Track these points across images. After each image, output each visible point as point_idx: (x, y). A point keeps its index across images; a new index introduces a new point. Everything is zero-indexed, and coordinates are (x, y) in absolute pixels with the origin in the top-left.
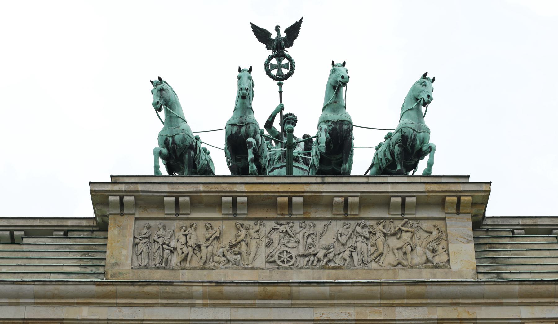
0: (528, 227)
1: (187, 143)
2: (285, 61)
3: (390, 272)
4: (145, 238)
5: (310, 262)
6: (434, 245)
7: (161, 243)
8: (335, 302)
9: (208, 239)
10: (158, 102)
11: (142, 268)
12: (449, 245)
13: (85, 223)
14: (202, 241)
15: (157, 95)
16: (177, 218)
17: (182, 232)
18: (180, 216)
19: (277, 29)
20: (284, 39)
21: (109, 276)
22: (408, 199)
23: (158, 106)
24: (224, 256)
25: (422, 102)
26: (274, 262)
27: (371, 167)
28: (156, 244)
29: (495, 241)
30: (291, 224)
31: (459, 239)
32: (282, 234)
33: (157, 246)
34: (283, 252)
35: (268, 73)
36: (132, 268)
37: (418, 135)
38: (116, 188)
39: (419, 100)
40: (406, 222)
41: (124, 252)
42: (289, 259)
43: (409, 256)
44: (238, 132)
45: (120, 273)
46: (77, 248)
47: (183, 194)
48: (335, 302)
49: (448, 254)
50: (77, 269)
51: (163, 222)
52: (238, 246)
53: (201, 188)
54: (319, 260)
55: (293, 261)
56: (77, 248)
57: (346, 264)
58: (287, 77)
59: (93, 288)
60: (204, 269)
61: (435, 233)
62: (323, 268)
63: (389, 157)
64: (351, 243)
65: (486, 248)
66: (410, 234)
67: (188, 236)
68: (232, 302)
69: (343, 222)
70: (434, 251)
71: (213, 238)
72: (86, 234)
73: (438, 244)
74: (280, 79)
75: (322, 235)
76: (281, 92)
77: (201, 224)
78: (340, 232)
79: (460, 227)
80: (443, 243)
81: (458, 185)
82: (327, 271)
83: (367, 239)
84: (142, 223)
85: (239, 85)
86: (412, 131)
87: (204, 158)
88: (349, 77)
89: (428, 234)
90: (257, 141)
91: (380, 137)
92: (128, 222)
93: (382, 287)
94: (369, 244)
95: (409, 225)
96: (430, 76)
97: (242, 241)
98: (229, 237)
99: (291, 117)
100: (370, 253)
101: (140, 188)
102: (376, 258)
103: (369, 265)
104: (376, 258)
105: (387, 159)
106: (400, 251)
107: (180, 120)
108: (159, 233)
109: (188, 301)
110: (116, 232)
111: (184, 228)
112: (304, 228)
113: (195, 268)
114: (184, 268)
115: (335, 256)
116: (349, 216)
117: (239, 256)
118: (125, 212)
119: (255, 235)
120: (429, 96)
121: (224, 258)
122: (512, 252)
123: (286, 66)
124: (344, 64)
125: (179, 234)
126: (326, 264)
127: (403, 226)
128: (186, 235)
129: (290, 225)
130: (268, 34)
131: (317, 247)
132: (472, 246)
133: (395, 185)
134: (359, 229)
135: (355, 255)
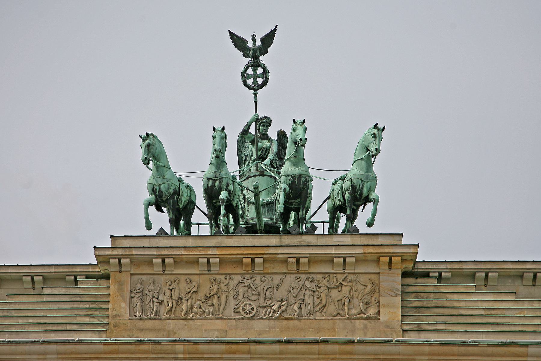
1: (171, 191)
2: (260, 71)
3: (331, 322)
7: (151, 297)
8: (283, 356)
9: (189, 293)
10: (146, 158)
11: (138, 319)
15: (145, 151)
17: (168, 287)
19: (254, 39)
20: (260, 48)
22: (348, 260)
23: (147, 162)
24: (200, 307)
27: (329, 198)
28: (148, 297)
30: (254, 279)
31: (389, 292)
32: (246, 288)
33: (148, 299)
34: (247, 304)
35: (245, 83)
36: (130, 319)
38: (115, 252)
40: (346, 277)
42: (251, 310)
43: (346, 308)
44: (213, 185)
47: (169, 257)
48: (283, 356)
49: (379, 306)
51: (152, 276)
52: (212, 298)
53: (182, 252)
54: (274, 311)
55: (254, 312)
57: (295, 316)
59: (102, 347)
60: (184, 319)
61: (369, 286)
62: (278, 319)
65: (412, 297)
66: (348, 288)
67: (173, 291)
68: (205, 356)
69: (296, 275)
70: (367, 303)
71: (192, 292)
74: (256, 88)
75: (278, 288)
76: (256, 102)
77: (183, 278)
78: (292, 286)
80: (376, 295)
83: (314, 292)
84: (136, 278)
87: (185, 196)
89: (365, 287)
90: (229, 192)
93: (319, 346)
94: (315, 295)
95: (348, 280)
97: (215, 294)
100: (315, 304)
101: (134, 252)
102: (320, 309)
103: (314, 314)
104: (320, 309)
105: (339, 201)
106: (340, 302)
107: (165, 169)
108: (149, 288)
109: (172, 356)
111: (169, 283)
112: (264, 282)
113: (178, 319)
114: (170, 319)
116: (300, 272)
117: (212, 307)
118: (123, 269)
119: (225, 289)
121: (200, 310)
123: (261, 76)
125: (165, 289)
128: (171, 290)
129: (252, 280)
130: (244, 42)
131: (274, 299)
134: (307, 284)
135: (303, 307)
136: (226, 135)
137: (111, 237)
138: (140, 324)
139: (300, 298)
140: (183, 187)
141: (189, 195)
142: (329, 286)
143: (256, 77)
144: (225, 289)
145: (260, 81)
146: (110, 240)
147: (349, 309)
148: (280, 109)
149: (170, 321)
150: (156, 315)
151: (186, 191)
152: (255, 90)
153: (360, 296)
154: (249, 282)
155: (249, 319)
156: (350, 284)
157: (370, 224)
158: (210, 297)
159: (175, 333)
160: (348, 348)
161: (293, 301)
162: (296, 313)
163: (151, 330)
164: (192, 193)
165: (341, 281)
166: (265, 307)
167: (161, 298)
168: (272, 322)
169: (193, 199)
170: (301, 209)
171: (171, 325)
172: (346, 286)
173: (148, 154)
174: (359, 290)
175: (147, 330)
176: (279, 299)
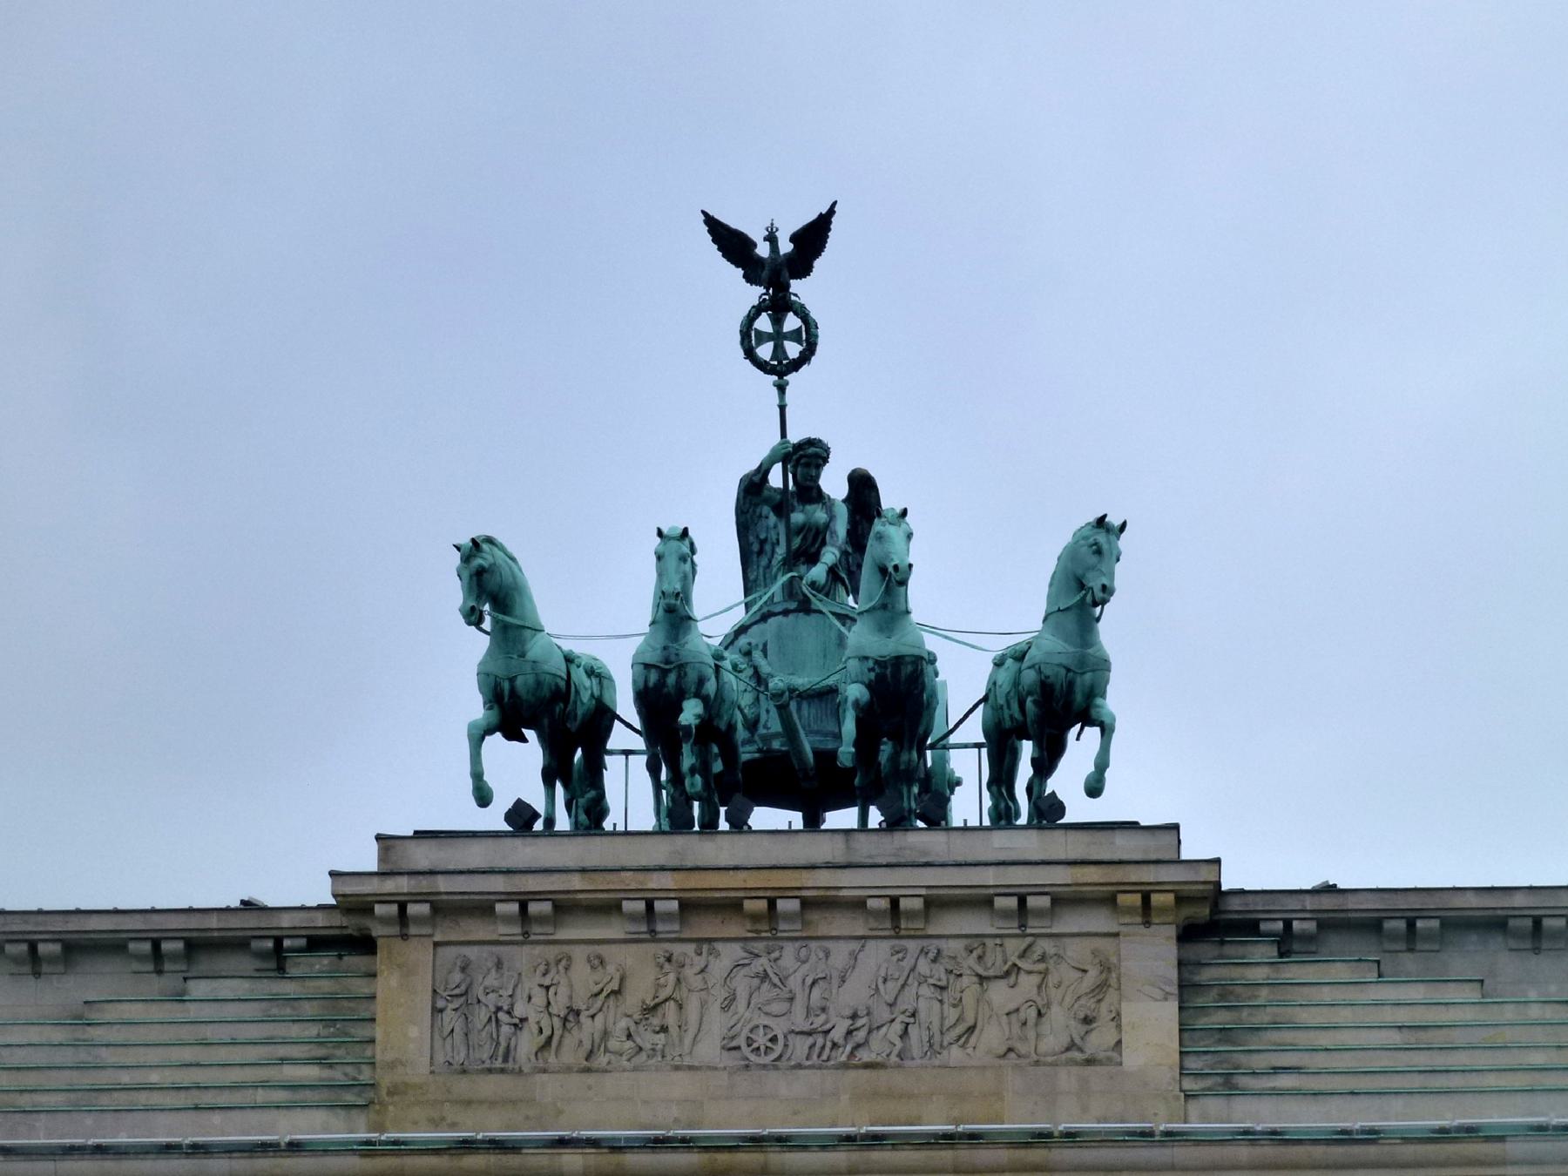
0: (1325, 915)
1: (546, 692)
2: (792, 322)
4: (456, 996)
5: (817, 1050)
6: (1087, 1005)
7: (493, 1009)
10: (473, 609)
12: (1123, 1005)
13: (320, 920)
14: (579, 1004)
16: (526, 938)
17: (538, 979)
18: (533, 938)
19: (771, 238)
21: (384, 1092)
25: (1089, 599)
26: (738, 1048)
27: (985, 699)
29: (1236, 972)
30: (776, 954)
32: (756, 981)
33: (482, 1015)
35: (750, 354)
36: (432, 1072)
37: (1078, 680)
38: (390, 885)
39: (1082, 588)
40: (1030, 946)
41: (413, 1032)
44: (661, 683)
45: (406, 1084)
46: (309, 1009)
47: (538, 896)
49: (1119, 1027)
50: (312, 1073)
51: (495, 949)
52: (660, 1011)
53: (576, 882)
55: (778, 1048)
56: (309, 1009)
58: (796, 365)
60: (588, 1070)
61: (1093, 973)
62: (845, 1066)
63: (1017, 715)
64: (907, 1002)
66: (1035, 979)
67: (552, 990)
70: (1087, 1020)
71: (604, 994)
72: (326, 961)
73: (1099, 1001)
74: (781, 369)
76: (782, 408)
77: (579, 953)
79: (1152, 955)
80: (1111, 996)
81: (1145, 867)
82: (852, 1074)
83: (942, 988)
84: (449, 953)
85: (660, 575)
86: (1063, 672)
88: (910, 566)
89: (1079, 974)
90: (705, 700)
91: (1001, 645)
92: (418, 953)
95: (1036, 957)
96: (1114, 520)
98: (639, 991)
99: (812, 450)
100: (948, 1023)
101: (443, 884)
102: (960, 1037)
103: (945, 1053)
104: (960, 1037)
105: (1011, 717)
106: (1014, 1017)
110: (394, 981)
111: (542, 968)
112: (804, 962)
113: (568, 1069)
114: (545, 1071)
115: (870, 1032)
116: (903, 933)
117: (662, 1035)
119: (696, 982)
120: (1104, 588)
121: (629, 1044)
122: (1269, 1009)
123: (795, 336)
124: (904, 513)
125: (531, 984)
126: (852, 1054)
127: (1023, 955)
128: (547, 988)
131: (832, 1011)
132: (1173, 1006)
133: (1002, 868)
134: (924, 966)
135: (912, 1030)
136: (692, 544)
137: (379, 838)
138: (462, 1086)
139: (902, 1008)
140: (579, 676)
141: (596, 693)
142: (984, 974)
143: (780, 338)
144: (696, 982)
145: (793, 350)
146: (373, 848)
147: (1038, 1036)
148: (850, 413)
149: (545, 1077)
150: (506, 1060)
151: (587, 683)
152: (781, 375)
153: (1068, 999)
154: (761, 964)
155: (764, 1066)
156: (1041, 966)
157: (1094, 788)
158: (656, 1007)
159: (560, 1112)
160: (1036, 1155)
161: (887, 1016)
162: (896, 1052)
163: (493, 1104)
164: (605, 682)
165: (1014, 959)
166: (809, 1034)
167: (519, 1010)
168: (829, 1079)
169: (607, 700)
170: (906, 745)
171: (548, 1088)
172: (1030, 972)
173: (479, 598)
174: (1066, 983)
175: (481, 1102)
176: (848, 1012)
